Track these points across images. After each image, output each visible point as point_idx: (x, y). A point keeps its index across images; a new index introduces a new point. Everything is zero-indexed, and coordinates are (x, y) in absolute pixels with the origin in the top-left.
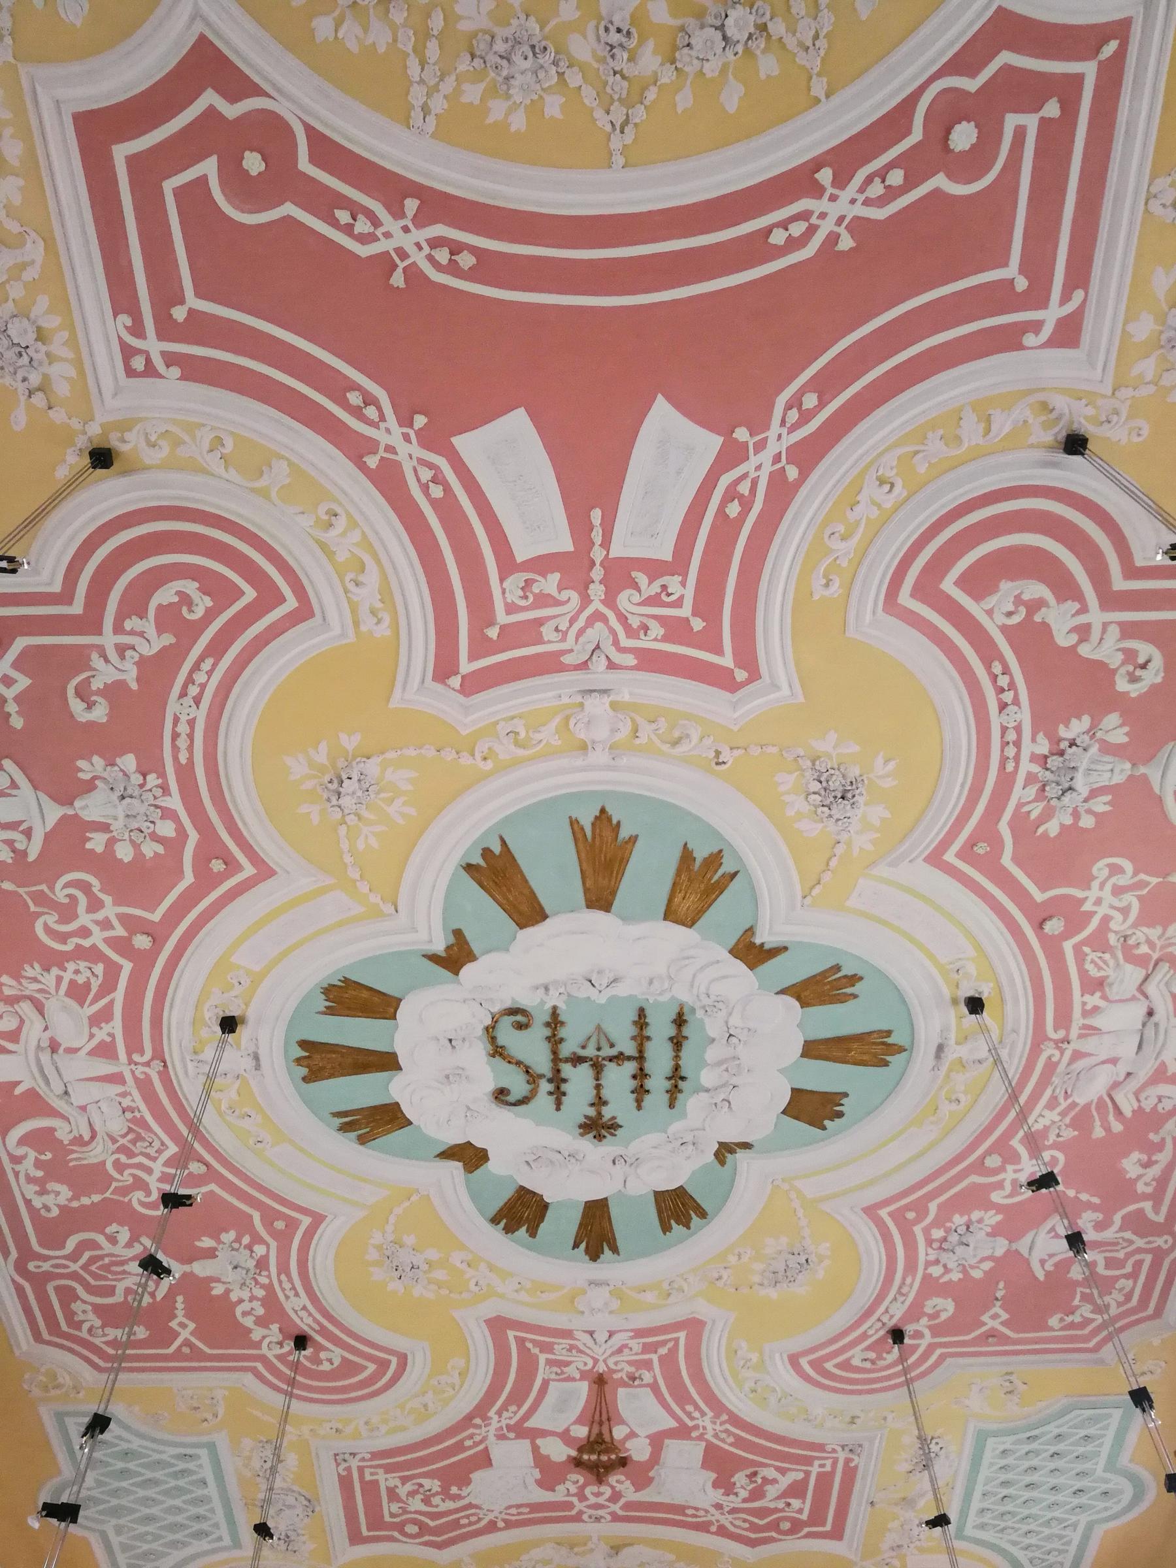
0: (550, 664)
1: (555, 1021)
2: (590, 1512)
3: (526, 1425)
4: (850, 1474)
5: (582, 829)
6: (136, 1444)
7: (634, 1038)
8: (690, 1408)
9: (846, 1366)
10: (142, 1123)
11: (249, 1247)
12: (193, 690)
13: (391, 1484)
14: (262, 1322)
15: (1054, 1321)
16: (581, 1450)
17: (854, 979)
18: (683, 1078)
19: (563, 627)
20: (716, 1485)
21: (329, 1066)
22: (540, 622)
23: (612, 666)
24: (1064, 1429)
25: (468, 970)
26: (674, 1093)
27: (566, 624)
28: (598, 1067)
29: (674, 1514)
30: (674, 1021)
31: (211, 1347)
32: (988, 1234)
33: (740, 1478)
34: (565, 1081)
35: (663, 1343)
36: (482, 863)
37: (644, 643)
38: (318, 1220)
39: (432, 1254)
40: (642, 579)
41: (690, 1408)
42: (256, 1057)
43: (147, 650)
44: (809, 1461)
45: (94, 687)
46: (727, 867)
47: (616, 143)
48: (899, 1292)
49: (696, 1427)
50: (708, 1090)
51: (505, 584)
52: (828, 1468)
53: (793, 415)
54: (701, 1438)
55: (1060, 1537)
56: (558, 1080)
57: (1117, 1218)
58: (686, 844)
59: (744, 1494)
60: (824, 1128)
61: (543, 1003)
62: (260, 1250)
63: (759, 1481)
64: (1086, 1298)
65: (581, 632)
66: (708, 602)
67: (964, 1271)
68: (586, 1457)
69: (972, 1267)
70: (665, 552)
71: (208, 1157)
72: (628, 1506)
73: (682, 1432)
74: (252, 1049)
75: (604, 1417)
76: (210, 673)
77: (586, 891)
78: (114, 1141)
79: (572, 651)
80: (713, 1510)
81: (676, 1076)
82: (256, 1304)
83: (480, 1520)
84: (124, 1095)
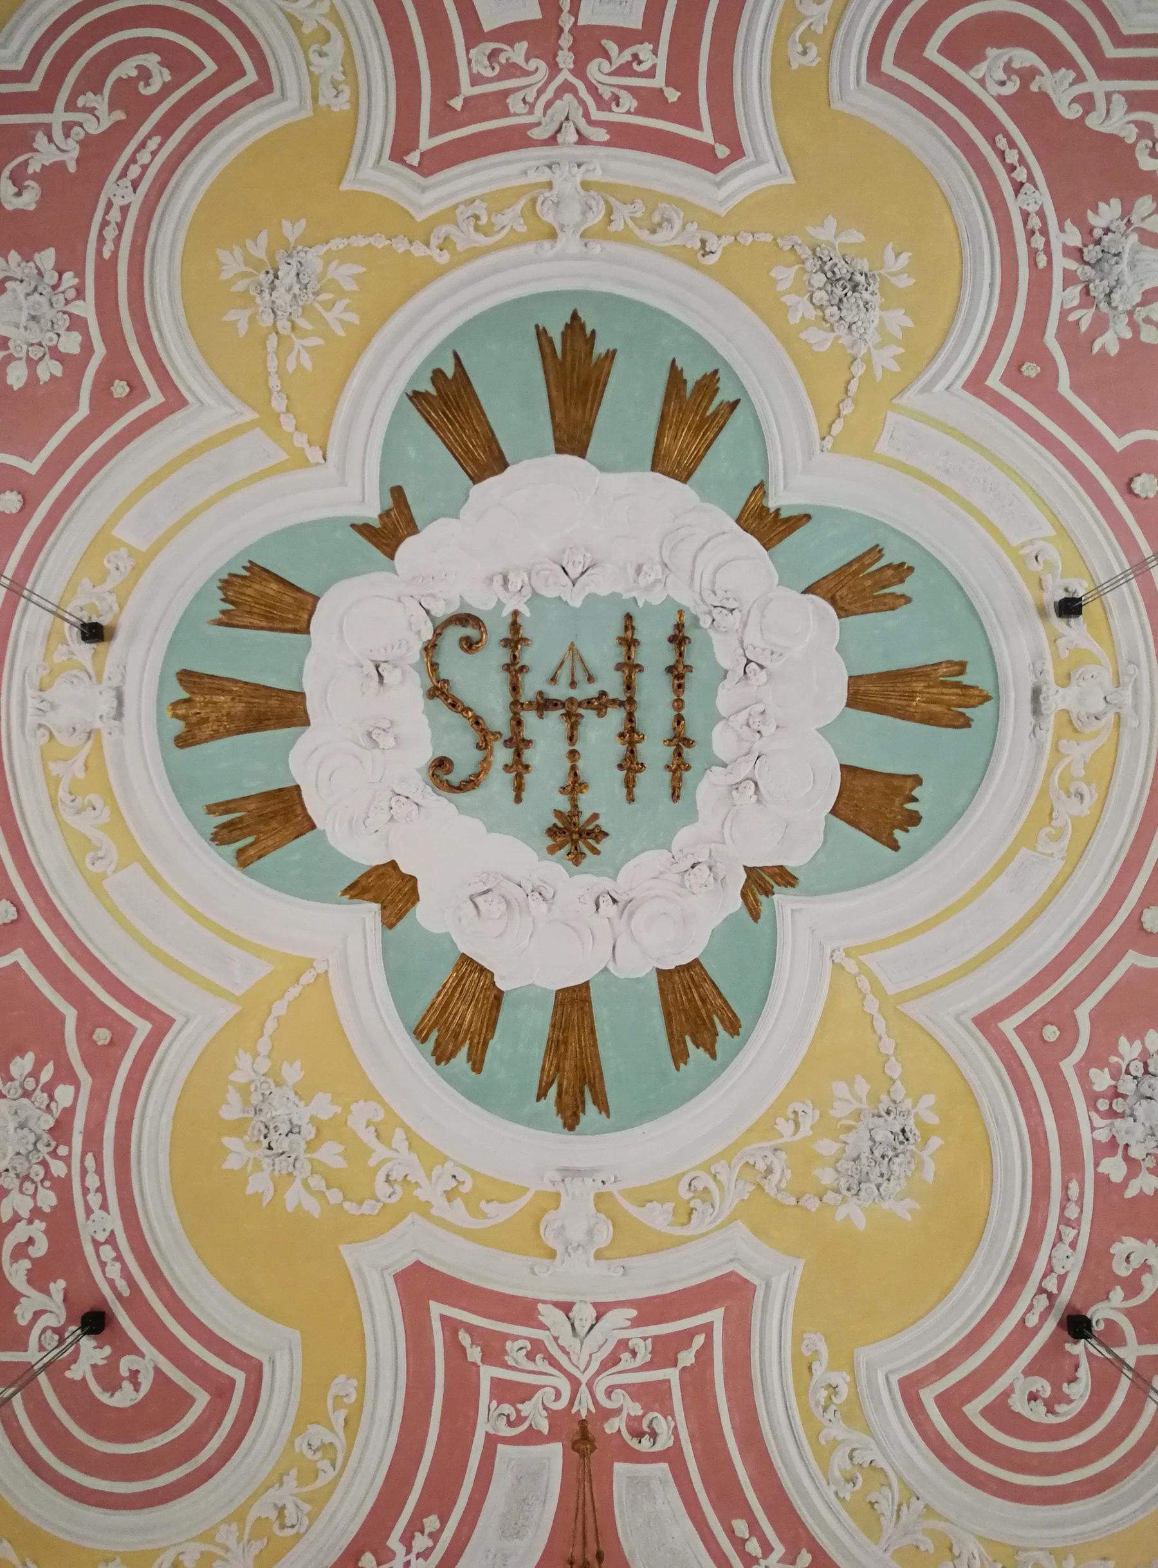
0: (515, 139)
1: (515, 640)
5: (551, 341)
7: (619, 667)
12: (134, 171)
17: (901, 571)
19: (530, 99)
21: (213, 716)
22: (506, 93)
23: (582, 140)
25: (408, 548)
26: (678, 768)
27: (533, 94)
28: (573, 720)
30: (672, 640)
34: (528, 743)
37: (617, 116)
39: (324, 1107)
40: (612, 47)
41: (741, 1527)
43: (93, 128)
45: (30, 171)
46: (725, 394)
48: (1064, 1221)
51: (473, 52)
56: (518, 743)
58: (674, 361)
61: (500, 605)
65: (549, 105)
66: (681, 69)
74: (116, 682)
76: (154, 154)
77: (556, 427)
79: (539, 124)
81: (680, 741)
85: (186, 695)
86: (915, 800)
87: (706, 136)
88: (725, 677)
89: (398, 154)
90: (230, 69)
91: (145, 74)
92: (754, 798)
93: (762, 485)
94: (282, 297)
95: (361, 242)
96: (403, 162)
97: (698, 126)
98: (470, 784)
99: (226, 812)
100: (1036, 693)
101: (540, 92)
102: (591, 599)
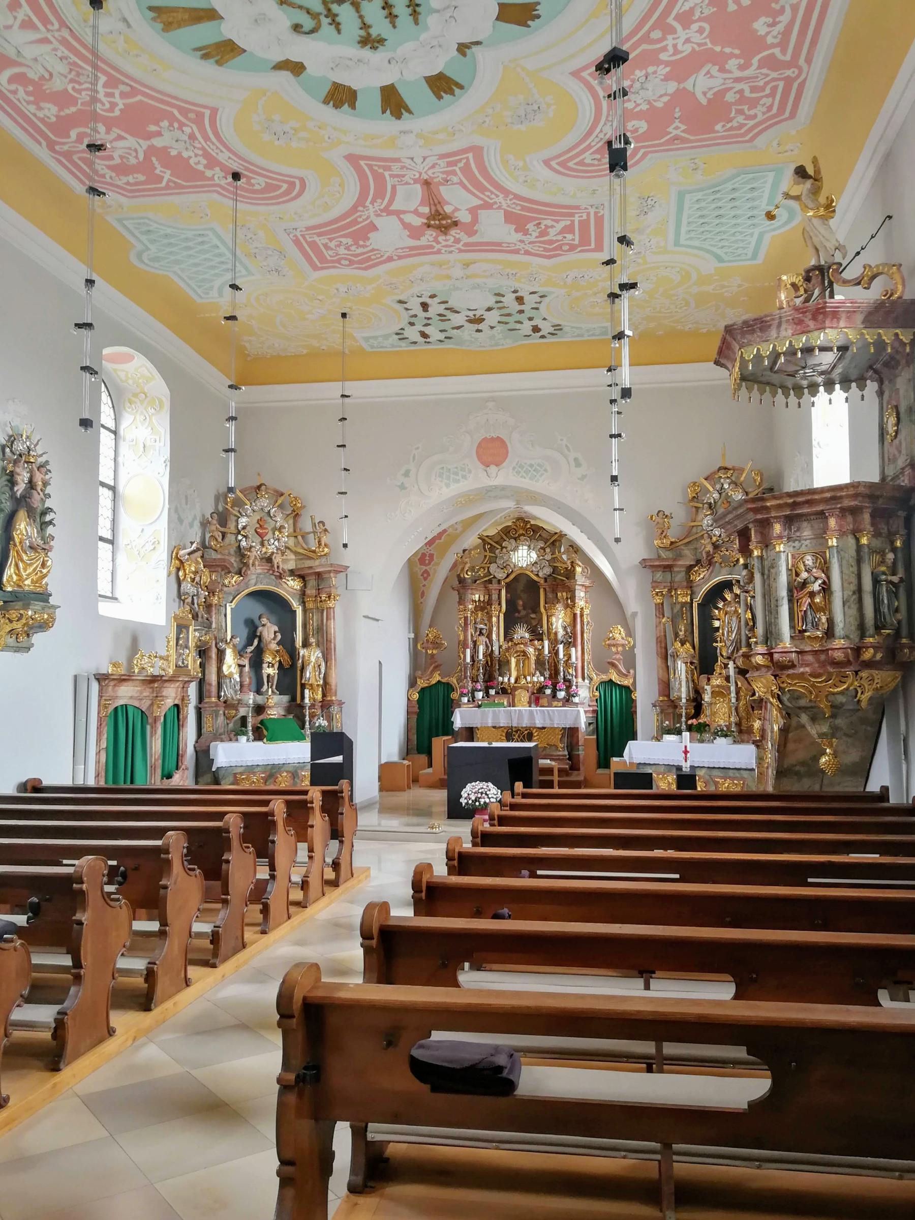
2: (445, 249)
3: (391, 208)
4: (599, 220)
6: (169, 231)
8: (488, 193)
9: (582, 163)
10: (75, 64)
11: (180, 128)
13: (324, 241)
14: (209, 166)
15: (718, 127)
16: (428, 219)
18: (418, 5)
20: (516, 231)
24: (736, 186)
26: (415, 14)
29: (495, 247)
31: (186, 181)
32: (662, 80)
33: (530, 226)
34: (337, 15)
35: (460, 160)
38: (214, 112)
42: (125, 20)
44: (572, 215)
48: (607, 120)
49: (495, 203)
50: (438, 11)
52: (585, 217)
54: (499, 208)
55: (743, 241)
57: (755, 61)
59: (535, 234)
60: (529, 26)
62: (187, 130)
63: (543, 227)
64: (740, 112)
67: (649, 103)
68: (432, 222)
69: (655, 101)
71: (127, 81)
72: (465, 245)
73: (487, 206)
75: (436, 201)
78: (66, 77)
80: (519, 243)
82: (201, 159)
83: (382, 256)
84: (55, 49)
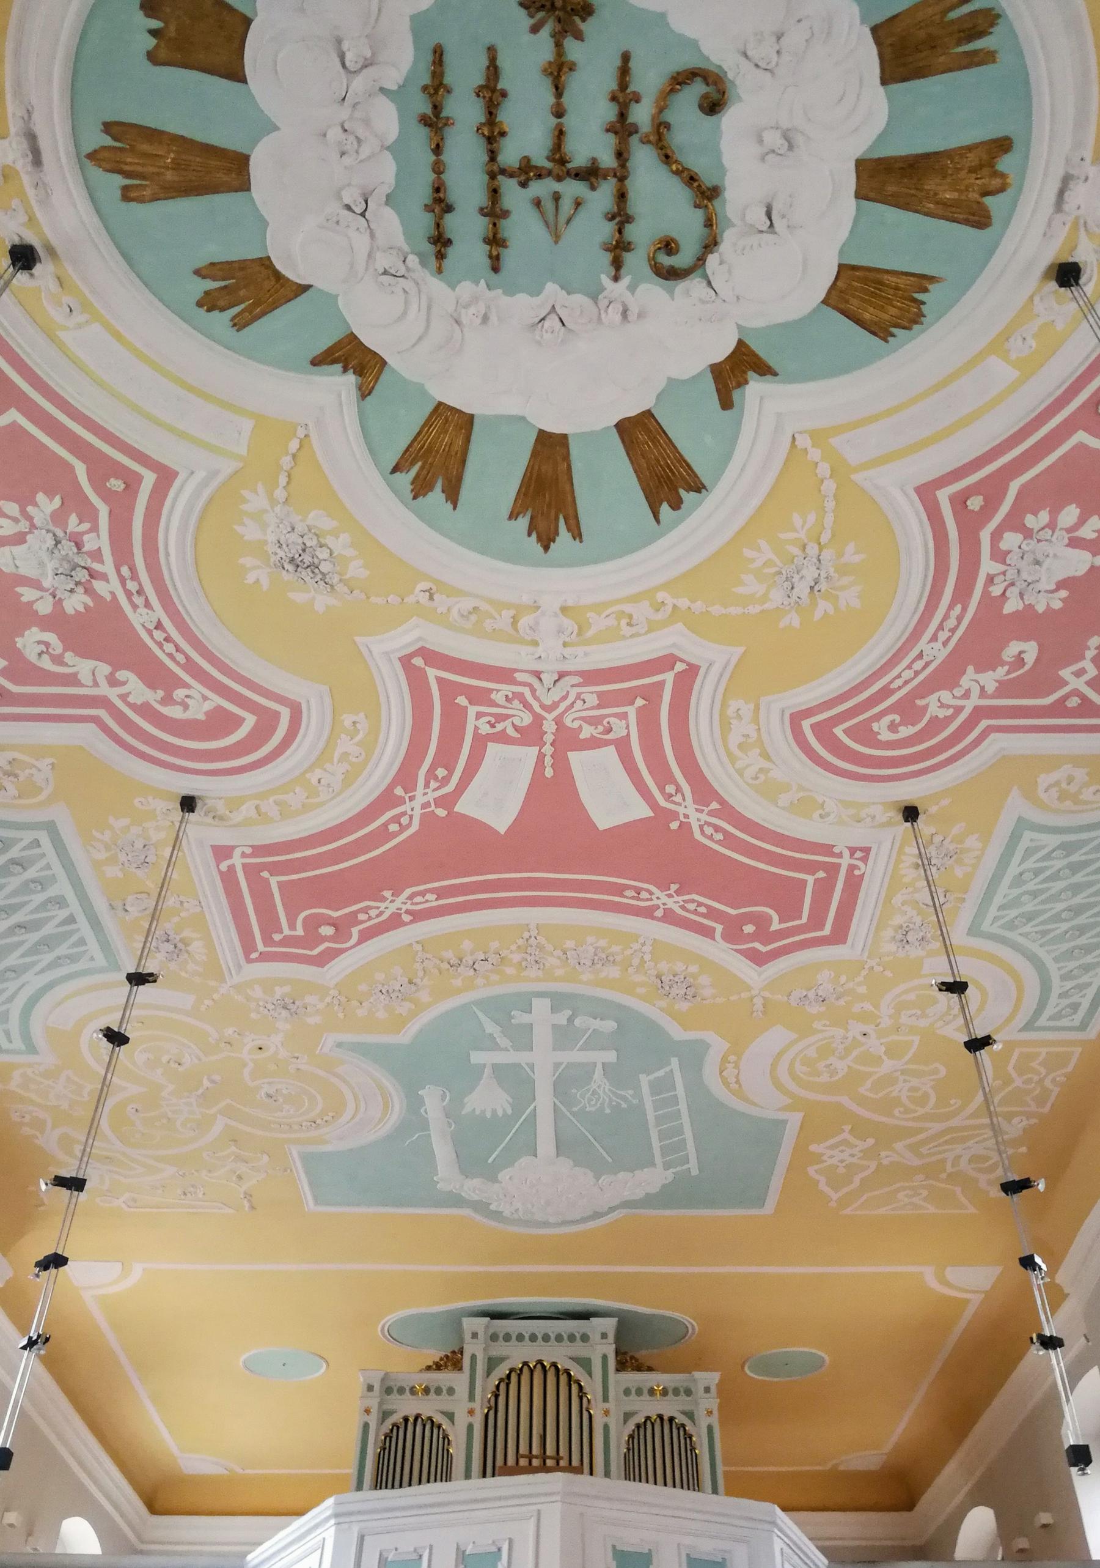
0: (590, 677)
1: (618, 251)
5: (569, 530)
7: (506, 214)
12: (918, 665)
19: (579, 703)
21: (963, 174)
23: (538, 675)
25: (722, 351)
26: (437, 88)
30: (449, 242)
36: (682, 492)
37: (507, 689)
40: (511, 731)
43: (945, 696)
45: (1006, 668)
46: (404, 479)
47: (534, 933)
51: (625, 733)
53: (405, 820)
56: (622, 128)
58: (455, 508)
61: (632, 288)
65: (564, 698)
66: (454, 720)
70: (492, 748)
76: (899, 676)
77: (567, 457)
79: (572, 686)
81: (435, 122)
85: (988, 201)
86: (153, 33)
87: (432, 673)
88: (388, 196)
89: (692, 671)
90: (823, 731)
91: (893, 728)
92: (345, 46)
93: (364, 396)
94: (810, 573)
95: (733, 610)
96: (688, 664)
97: (439, 680)
98: (681, 79)
99: (975, 53)
100: (37, 160)
101: (572, 705)
102: (536, 292)
